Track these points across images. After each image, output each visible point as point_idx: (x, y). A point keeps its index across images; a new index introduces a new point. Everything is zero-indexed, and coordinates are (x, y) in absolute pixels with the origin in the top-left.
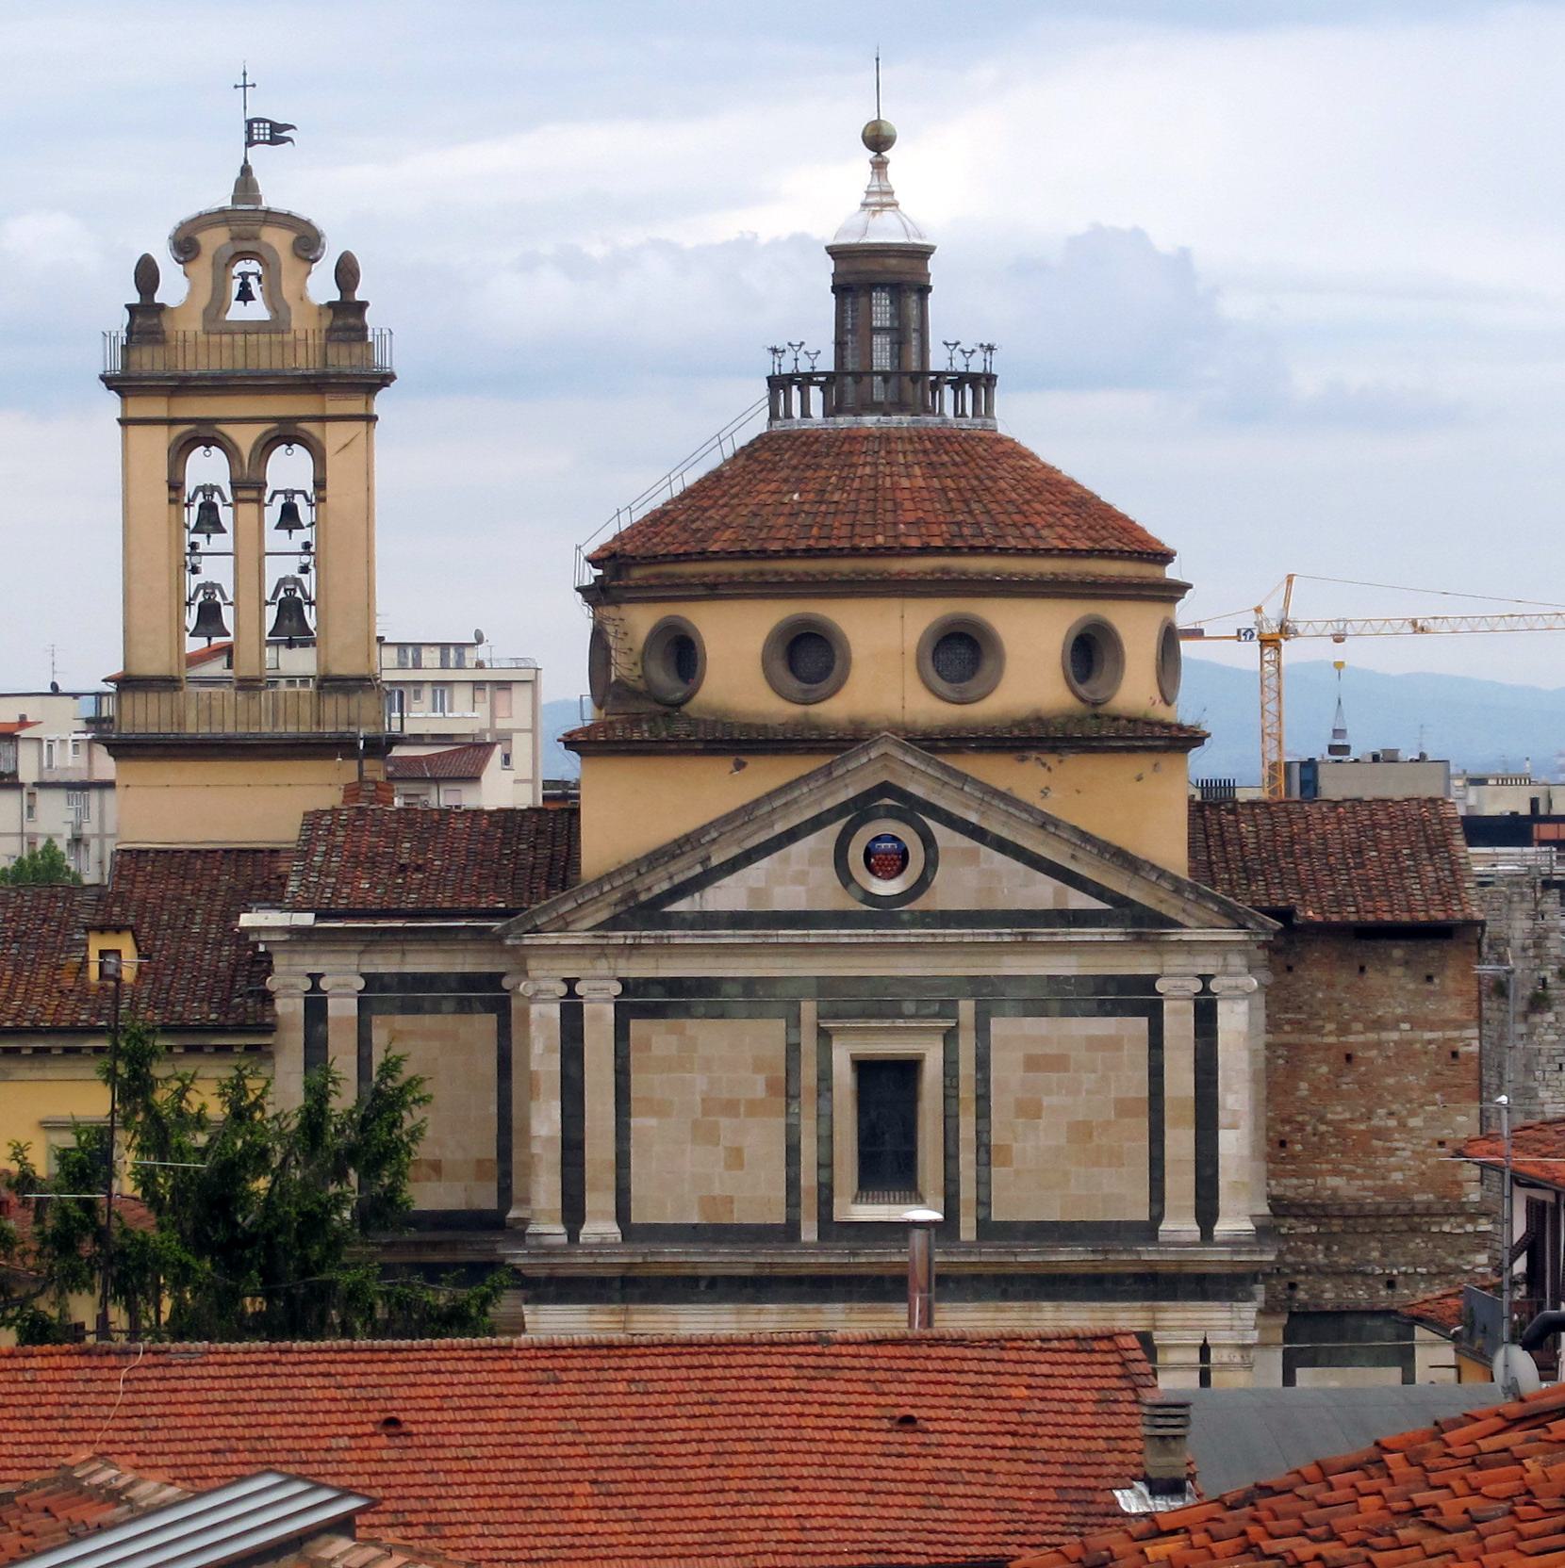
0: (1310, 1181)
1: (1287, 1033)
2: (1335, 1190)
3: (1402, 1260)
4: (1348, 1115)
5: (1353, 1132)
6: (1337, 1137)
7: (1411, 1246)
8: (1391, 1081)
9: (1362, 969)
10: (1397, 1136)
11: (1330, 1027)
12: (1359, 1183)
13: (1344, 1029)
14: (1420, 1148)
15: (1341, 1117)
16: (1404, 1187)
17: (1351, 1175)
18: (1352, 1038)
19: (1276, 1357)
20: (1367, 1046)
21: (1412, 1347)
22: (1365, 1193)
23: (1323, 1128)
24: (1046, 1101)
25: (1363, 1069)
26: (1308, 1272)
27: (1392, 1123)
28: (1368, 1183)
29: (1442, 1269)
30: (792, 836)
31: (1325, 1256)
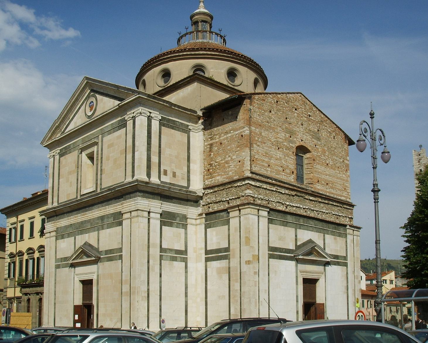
0: (213, 179)
1: (209, 141)
2: (218, 180)
3: (230, 196)
4: (221, 159)
5: (222, 163)
6: (219, 165)
7: (232, 191)
8: (229, 147)
9: (223, 120)
10: (230, 162)
11: (217, 137)
12: (223, 177)
13: (220, 137)
14: (235, 164)
15: (219, 160)
16: (232, 175)
17: (222, 175)
18: (221, 138)
19: (203, 226)
20: (224, 140)
21: (229, 219)
22: (224, 179)
23: (216, 164)
24: (111, 155)
25: (224, 146)
26: (211, 203)
27: (230, 159)
28: (225, 176)
29: (238, 196)
30: (80, 108)
31: (215, 198)
